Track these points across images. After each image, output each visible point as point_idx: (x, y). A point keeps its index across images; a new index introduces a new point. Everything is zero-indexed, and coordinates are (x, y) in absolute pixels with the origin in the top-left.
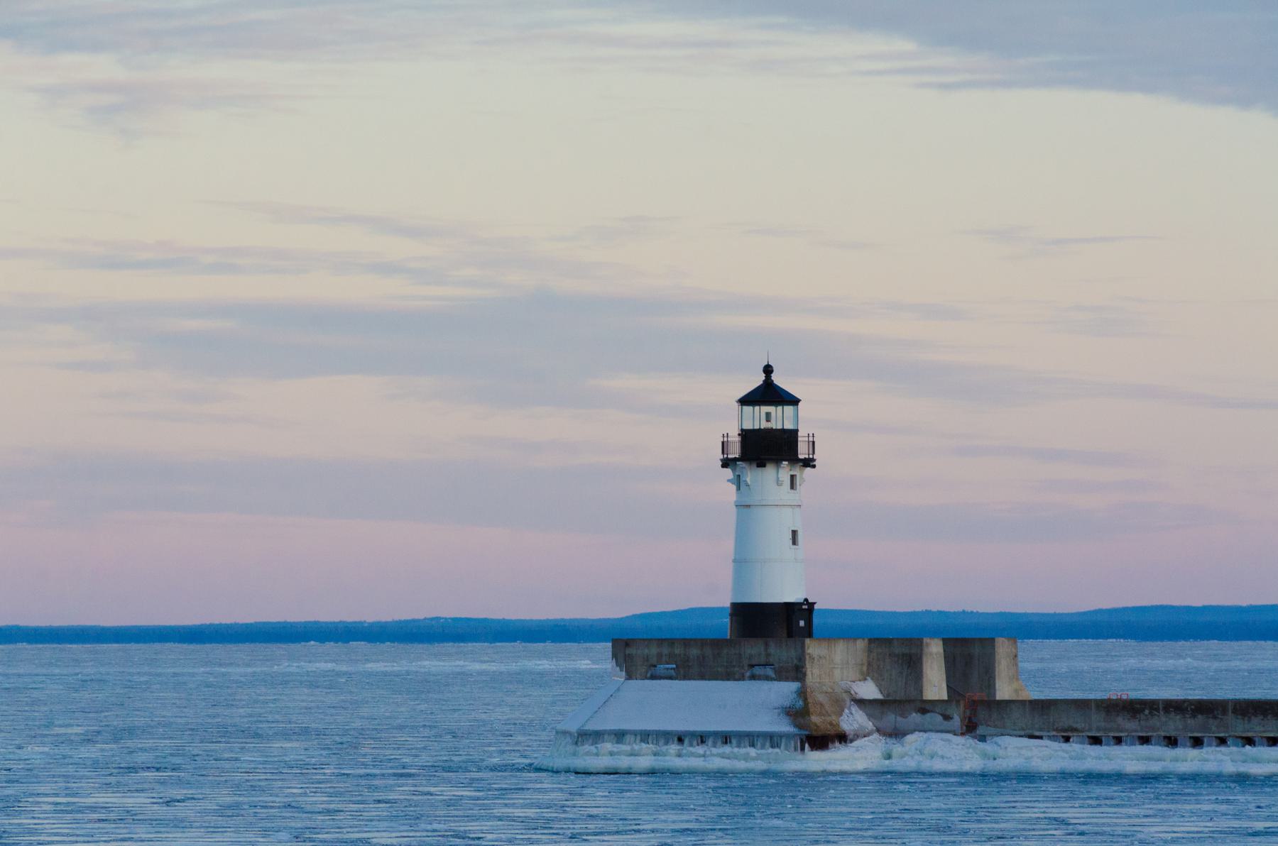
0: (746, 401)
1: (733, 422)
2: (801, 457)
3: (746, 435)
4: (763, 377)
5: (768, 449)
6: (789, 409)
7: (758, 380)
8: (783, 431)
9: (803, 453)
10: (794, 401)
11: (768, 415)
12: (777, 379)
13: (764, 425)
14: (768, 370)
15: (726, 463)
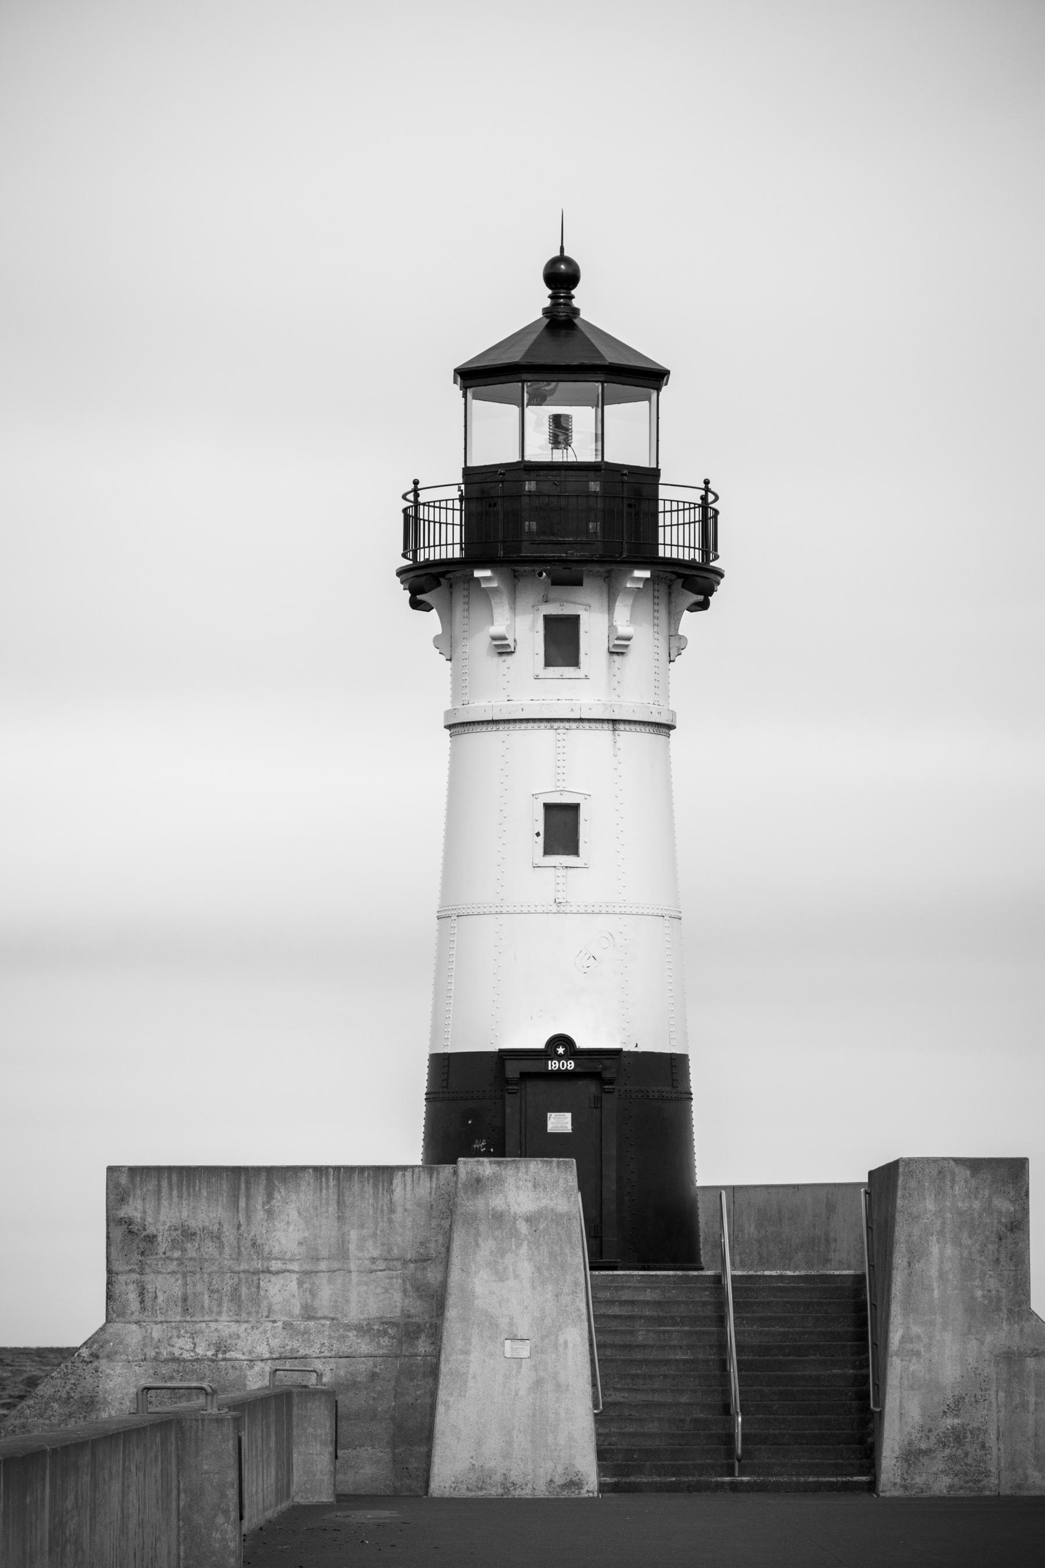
2: (663, 552)
4: (539, 298)
5: (559, 532)
10: (649, 378)
12: (589, 303)
14: (562, 277)
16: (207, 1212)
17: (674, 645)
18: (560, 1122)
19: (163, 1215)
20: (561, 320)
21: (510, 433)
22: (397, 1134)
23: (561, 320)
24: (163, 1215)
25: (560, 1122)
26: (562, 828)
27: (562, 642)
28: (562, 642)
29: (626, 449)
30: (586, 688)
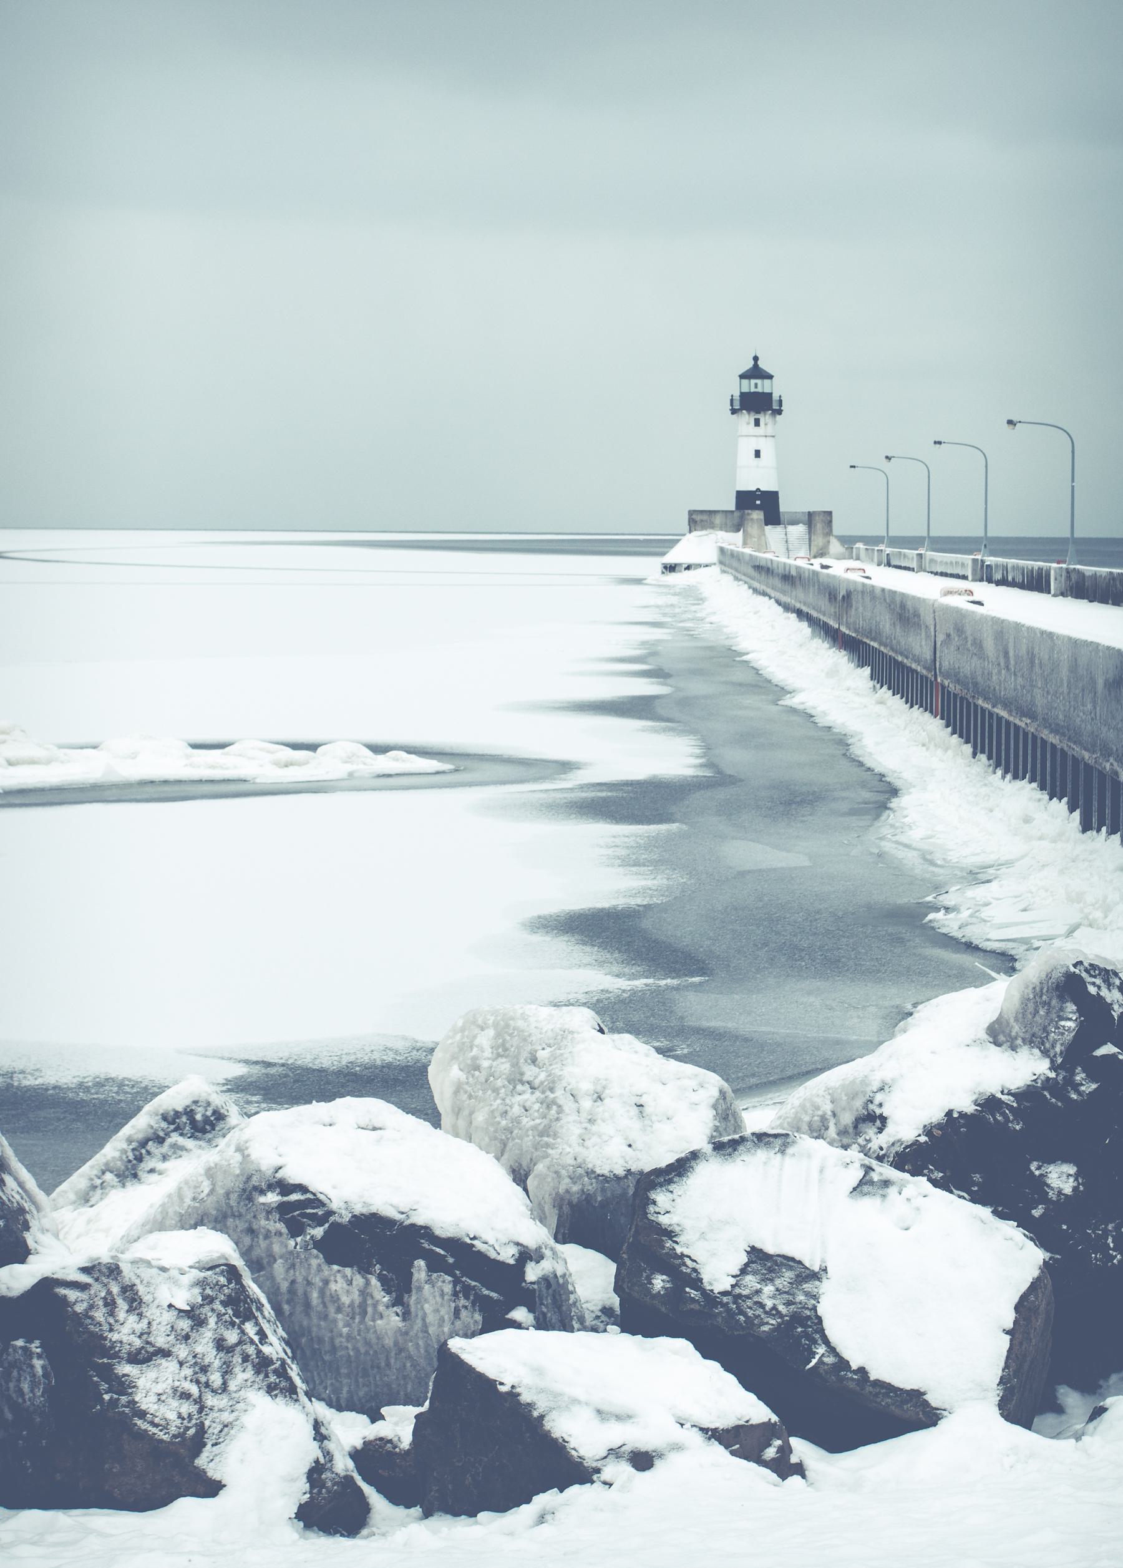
0: (742, 377)
1: (736, 388)
3: (742, 395)
4: (752, 362)
6: (767, 382)
7: (751, 363)
8: (763, 393)
9: (775, 407)
10: (771, 377)
11: (756, 386)
12: (761, 364)
13: (753, 390)
14: (756, 359)
15: (734, 411)
16: (705, 517)
17: (775, 423)
18: (758, 502)
19: (698, 518)
20: (756, 365)
21: (750, 386)
22: (731, 505)
23: (756, 365)
24: (698, 518)
25: (758, 502)
26: (758, 454)
27: (757, 423)
28: (757, 423)
29: (767, 390)
30: (760, 430)
